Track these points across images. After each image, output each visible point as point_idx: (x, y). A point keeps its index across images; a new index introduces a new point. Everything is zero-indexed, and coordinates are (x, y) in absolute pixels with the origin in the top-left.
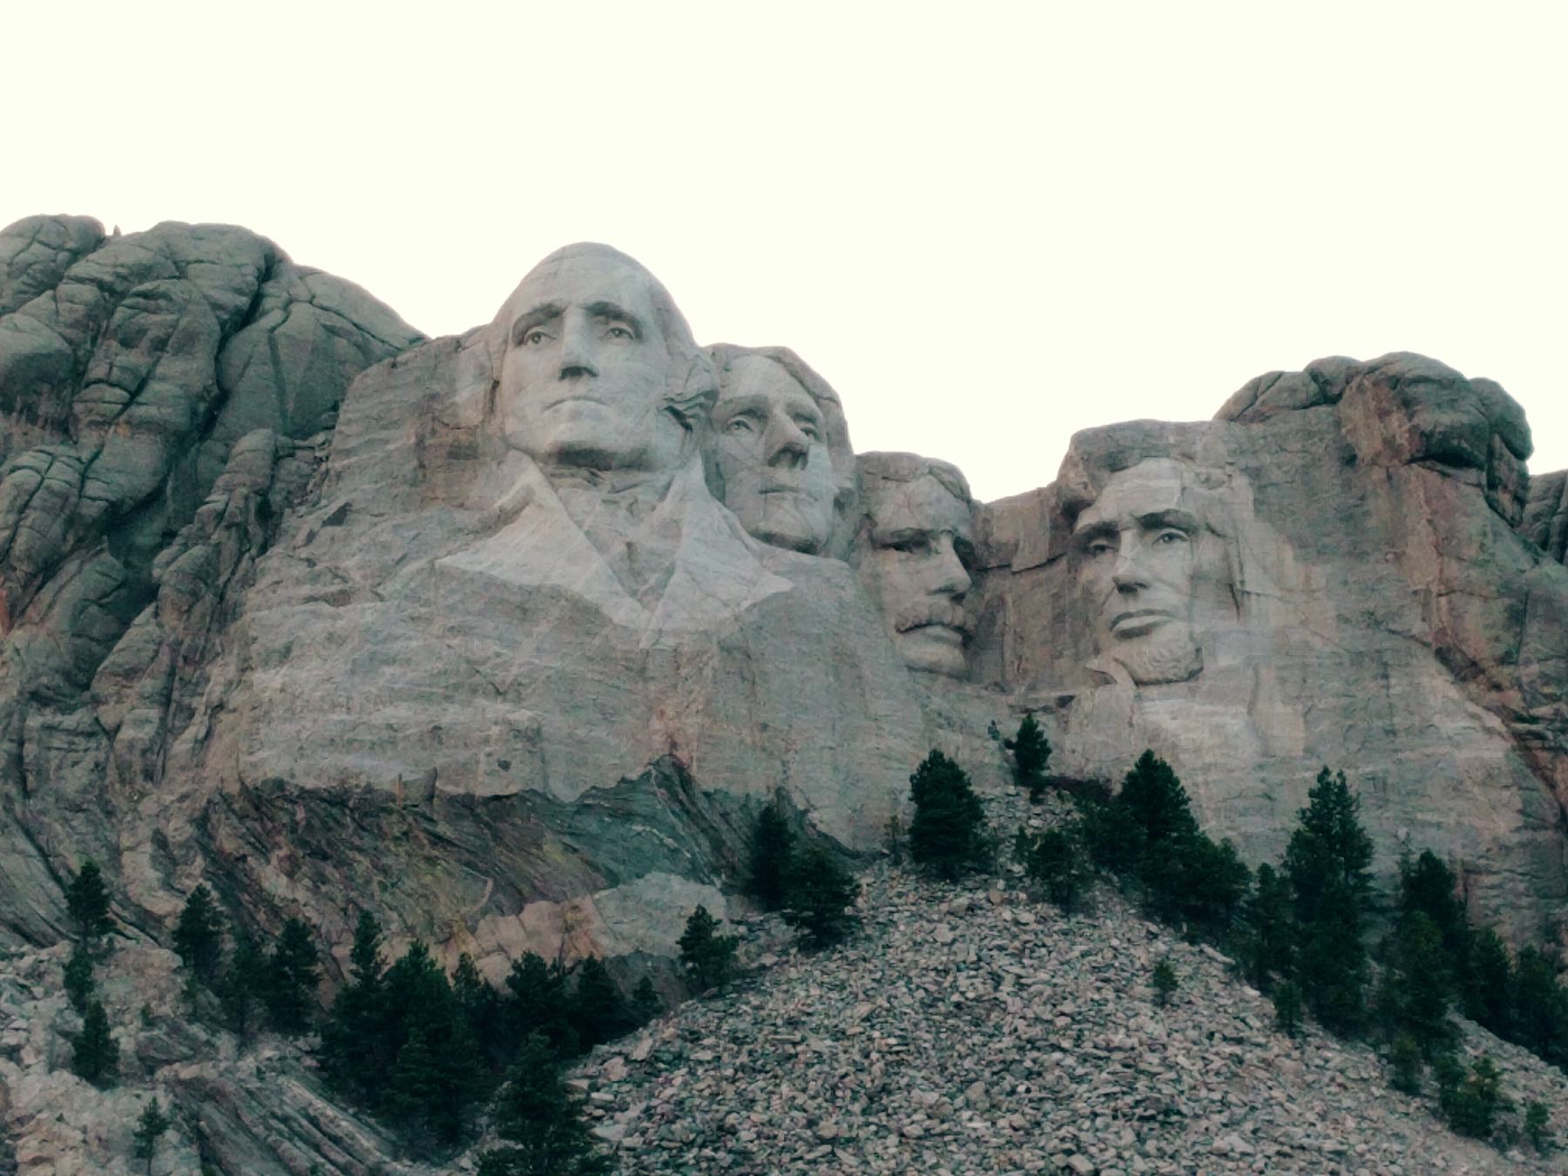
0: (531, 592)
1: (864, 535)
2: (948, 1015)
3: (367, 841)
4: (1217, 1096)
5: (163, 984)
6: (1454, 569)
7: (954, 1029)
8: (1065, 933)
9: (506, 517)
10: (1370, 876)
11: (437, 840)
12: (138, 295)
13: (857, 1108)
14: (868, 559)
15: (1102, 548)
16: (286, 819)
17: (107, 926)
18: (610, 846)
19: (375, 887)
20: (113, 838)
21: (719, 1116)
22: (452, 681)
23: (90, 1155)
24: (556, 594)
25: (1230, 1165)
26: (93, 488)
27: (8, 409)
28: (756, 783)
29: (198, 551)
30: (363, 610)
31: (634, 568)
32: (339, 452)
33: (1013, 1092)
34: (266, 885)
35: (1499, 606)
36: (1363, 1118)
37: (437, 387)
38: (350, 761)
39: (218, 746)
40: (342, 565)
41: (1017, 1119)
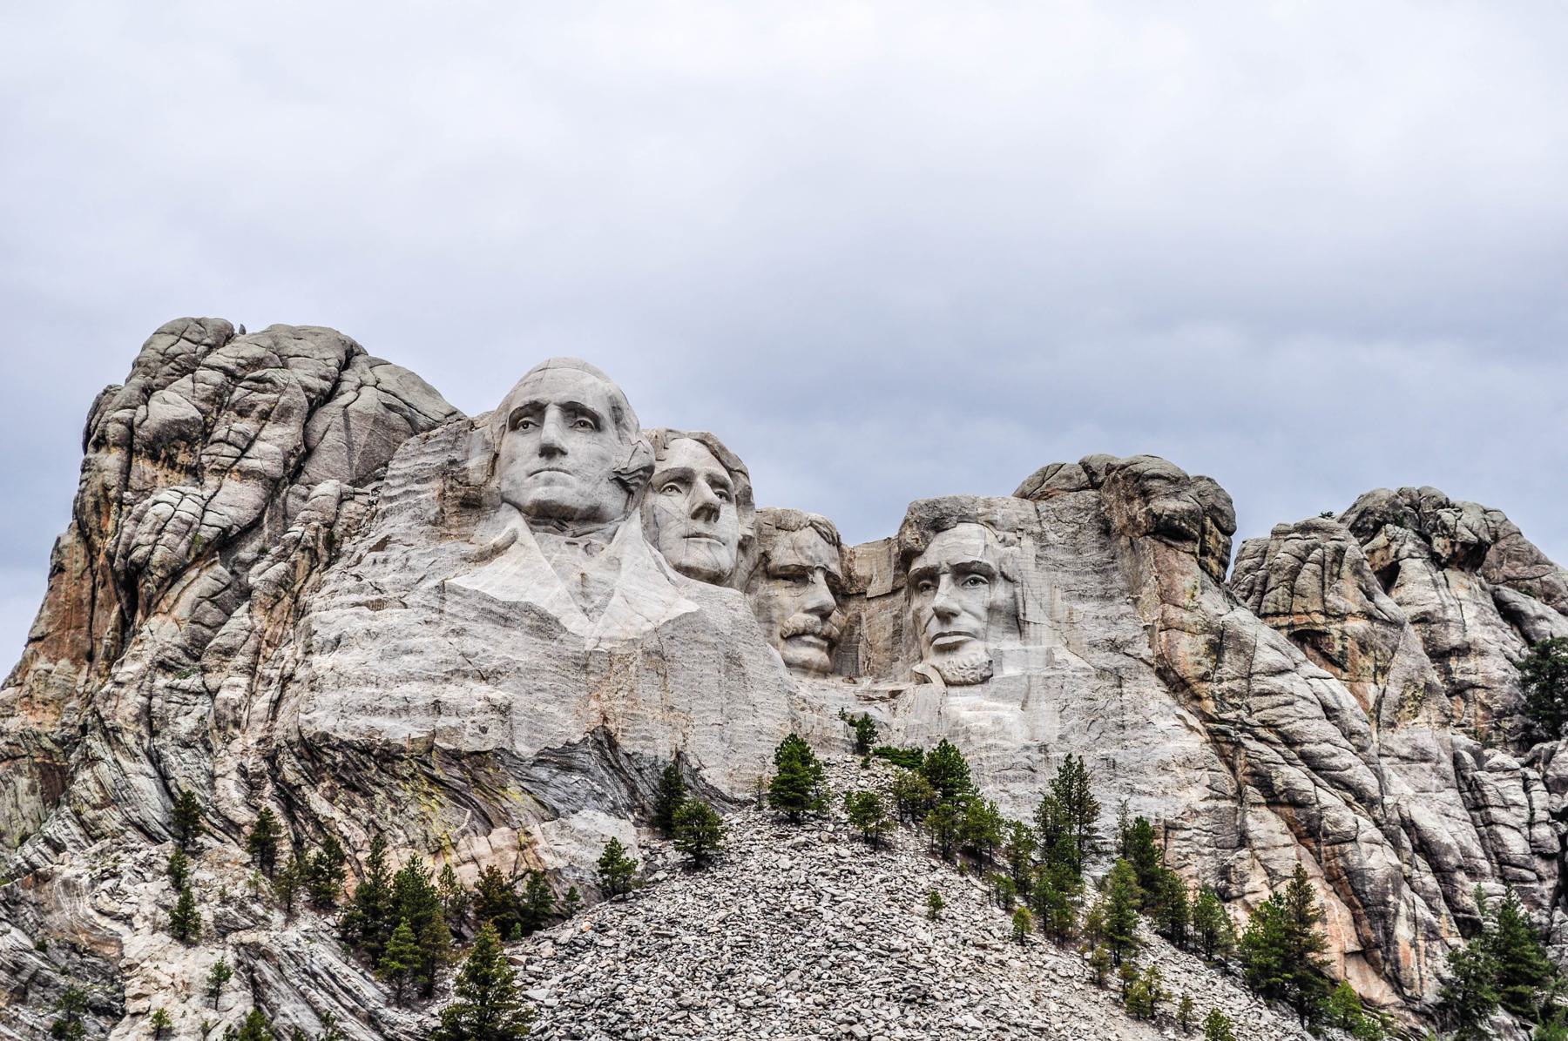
0: (512, 606)
1: (761, 568)
2: (780, 921)
3: (385, 779)
5: (236, 874)
6: (1173, 613)
7: (784, 931)
8: (871, 864)
9: (497, 551)
10: (1096, 830)
11: (434, 781)
12: (250, 379)
13: (709, 985)
14: (764, 587)
15: (928, 587)
16: (329, 761)
17: (199, 830)
18: (554, 791)
19: (388, 811)
20: (210, 767)
22: (451, 668)
23: (177, 993)
24: (528, 609)
26: (210, 518)
33: (819, 978)
34: (313, 806)
35: (1202, 639)
37: (456, 455)
38: (378, 722)
39: (285, 707)
40: (380, 580)
41: (820, 998)
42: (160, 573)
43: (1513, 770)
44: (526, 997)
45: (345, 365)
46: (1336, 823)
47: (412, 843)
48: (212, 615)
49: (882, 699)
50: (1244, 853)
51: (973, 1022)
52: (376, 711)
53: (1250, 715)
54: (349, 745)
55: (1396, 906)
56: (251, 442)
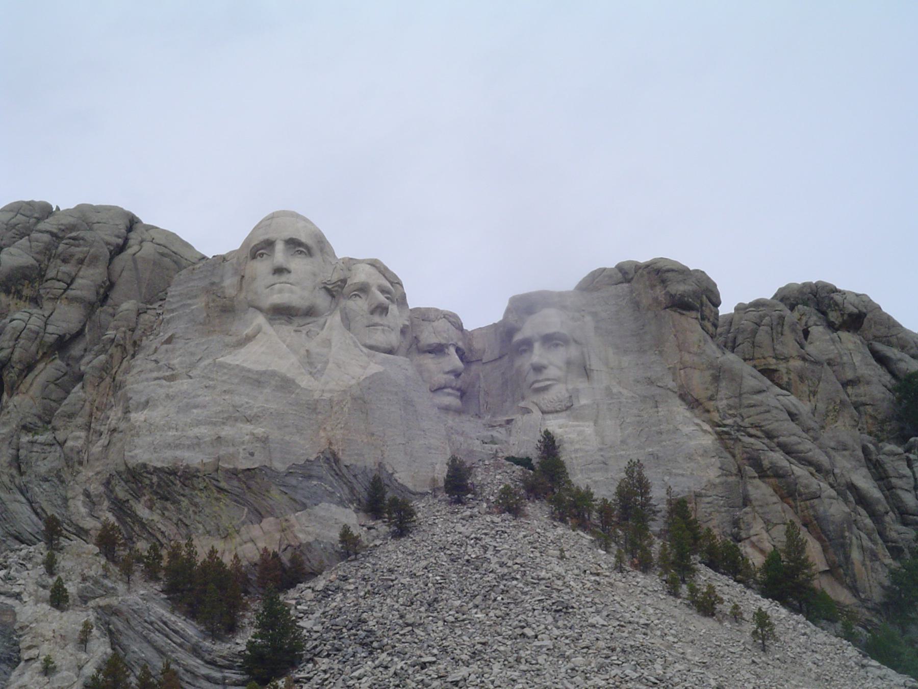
0: (264, 373)
1: (414, 347)
3: (187, 491)
4: (589, 600)
5: (90, 561)
6: (687, 357)
8: (514, 526)
9: (249, 339)
11: (221, 490)
12: (70, 238)
15: (525, 351)
16: (148, 482)
17: (60, 534)
19: (191, 512)
20: (63, 493)
21: (358, 614)
22: (226, 415)
24: (274, 374)
25: (598, 631)
26: (50, 329)
27: (8, 292)
28: (369, 461)
29: (103, 357)
30: (182, 383)
32: (168, 311)
33: (495, 600)
34: (139, 513)
35: (708, 373)
36: (657, 609)
37: (216, 280)
38: (179, 453)
41: (498, 613)
42: (19, 366)
43: (900, 454)
44: (299, 627)
45: (130, 229)
46: (806, 487)
47: (209, 532)
48: (56, 393)
49: (500, 426)
50: (748, 509)
51: (602, 622)
52: (177, 447)
53: (743, 420)
54: (161, 470)
55: (850, 539)
56: (73, 280)
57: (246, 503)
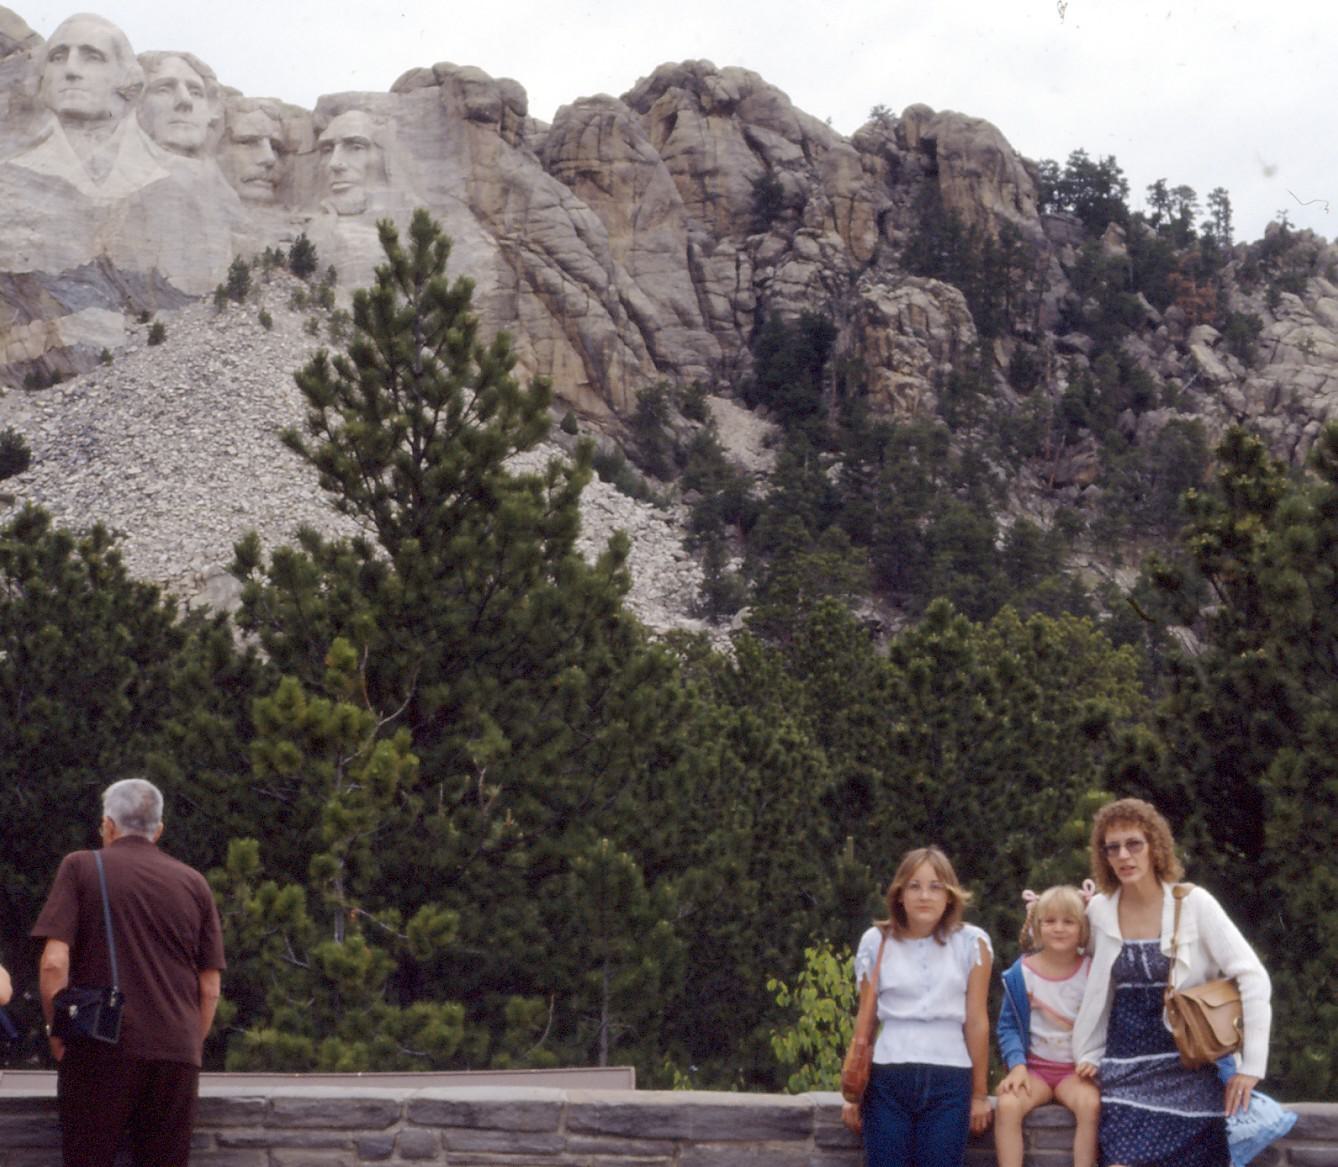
0: (47, 178)
6: (479, 170)
24: (58, 179)
31: (95, 169)
35: (498, 187)
43: (730, 255)
46: (574, 305)
57: (17, 305)
